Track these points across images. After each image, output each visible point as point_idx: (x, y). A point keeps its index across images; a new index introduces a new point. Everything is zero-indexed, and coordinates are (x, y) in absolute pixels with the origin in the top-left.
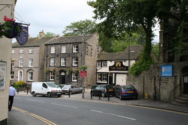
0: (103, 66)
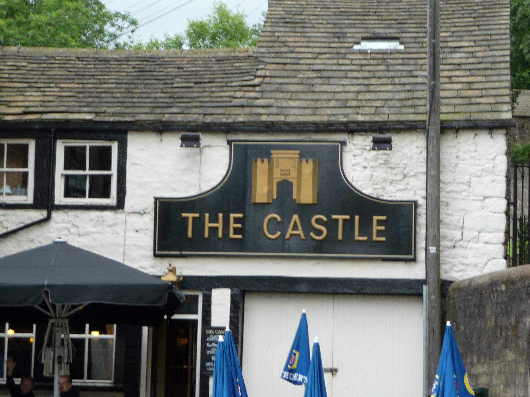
0: (59, 197)
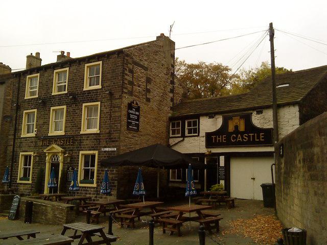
0: (186, 134)
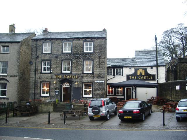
0: (116, 75)
